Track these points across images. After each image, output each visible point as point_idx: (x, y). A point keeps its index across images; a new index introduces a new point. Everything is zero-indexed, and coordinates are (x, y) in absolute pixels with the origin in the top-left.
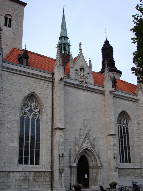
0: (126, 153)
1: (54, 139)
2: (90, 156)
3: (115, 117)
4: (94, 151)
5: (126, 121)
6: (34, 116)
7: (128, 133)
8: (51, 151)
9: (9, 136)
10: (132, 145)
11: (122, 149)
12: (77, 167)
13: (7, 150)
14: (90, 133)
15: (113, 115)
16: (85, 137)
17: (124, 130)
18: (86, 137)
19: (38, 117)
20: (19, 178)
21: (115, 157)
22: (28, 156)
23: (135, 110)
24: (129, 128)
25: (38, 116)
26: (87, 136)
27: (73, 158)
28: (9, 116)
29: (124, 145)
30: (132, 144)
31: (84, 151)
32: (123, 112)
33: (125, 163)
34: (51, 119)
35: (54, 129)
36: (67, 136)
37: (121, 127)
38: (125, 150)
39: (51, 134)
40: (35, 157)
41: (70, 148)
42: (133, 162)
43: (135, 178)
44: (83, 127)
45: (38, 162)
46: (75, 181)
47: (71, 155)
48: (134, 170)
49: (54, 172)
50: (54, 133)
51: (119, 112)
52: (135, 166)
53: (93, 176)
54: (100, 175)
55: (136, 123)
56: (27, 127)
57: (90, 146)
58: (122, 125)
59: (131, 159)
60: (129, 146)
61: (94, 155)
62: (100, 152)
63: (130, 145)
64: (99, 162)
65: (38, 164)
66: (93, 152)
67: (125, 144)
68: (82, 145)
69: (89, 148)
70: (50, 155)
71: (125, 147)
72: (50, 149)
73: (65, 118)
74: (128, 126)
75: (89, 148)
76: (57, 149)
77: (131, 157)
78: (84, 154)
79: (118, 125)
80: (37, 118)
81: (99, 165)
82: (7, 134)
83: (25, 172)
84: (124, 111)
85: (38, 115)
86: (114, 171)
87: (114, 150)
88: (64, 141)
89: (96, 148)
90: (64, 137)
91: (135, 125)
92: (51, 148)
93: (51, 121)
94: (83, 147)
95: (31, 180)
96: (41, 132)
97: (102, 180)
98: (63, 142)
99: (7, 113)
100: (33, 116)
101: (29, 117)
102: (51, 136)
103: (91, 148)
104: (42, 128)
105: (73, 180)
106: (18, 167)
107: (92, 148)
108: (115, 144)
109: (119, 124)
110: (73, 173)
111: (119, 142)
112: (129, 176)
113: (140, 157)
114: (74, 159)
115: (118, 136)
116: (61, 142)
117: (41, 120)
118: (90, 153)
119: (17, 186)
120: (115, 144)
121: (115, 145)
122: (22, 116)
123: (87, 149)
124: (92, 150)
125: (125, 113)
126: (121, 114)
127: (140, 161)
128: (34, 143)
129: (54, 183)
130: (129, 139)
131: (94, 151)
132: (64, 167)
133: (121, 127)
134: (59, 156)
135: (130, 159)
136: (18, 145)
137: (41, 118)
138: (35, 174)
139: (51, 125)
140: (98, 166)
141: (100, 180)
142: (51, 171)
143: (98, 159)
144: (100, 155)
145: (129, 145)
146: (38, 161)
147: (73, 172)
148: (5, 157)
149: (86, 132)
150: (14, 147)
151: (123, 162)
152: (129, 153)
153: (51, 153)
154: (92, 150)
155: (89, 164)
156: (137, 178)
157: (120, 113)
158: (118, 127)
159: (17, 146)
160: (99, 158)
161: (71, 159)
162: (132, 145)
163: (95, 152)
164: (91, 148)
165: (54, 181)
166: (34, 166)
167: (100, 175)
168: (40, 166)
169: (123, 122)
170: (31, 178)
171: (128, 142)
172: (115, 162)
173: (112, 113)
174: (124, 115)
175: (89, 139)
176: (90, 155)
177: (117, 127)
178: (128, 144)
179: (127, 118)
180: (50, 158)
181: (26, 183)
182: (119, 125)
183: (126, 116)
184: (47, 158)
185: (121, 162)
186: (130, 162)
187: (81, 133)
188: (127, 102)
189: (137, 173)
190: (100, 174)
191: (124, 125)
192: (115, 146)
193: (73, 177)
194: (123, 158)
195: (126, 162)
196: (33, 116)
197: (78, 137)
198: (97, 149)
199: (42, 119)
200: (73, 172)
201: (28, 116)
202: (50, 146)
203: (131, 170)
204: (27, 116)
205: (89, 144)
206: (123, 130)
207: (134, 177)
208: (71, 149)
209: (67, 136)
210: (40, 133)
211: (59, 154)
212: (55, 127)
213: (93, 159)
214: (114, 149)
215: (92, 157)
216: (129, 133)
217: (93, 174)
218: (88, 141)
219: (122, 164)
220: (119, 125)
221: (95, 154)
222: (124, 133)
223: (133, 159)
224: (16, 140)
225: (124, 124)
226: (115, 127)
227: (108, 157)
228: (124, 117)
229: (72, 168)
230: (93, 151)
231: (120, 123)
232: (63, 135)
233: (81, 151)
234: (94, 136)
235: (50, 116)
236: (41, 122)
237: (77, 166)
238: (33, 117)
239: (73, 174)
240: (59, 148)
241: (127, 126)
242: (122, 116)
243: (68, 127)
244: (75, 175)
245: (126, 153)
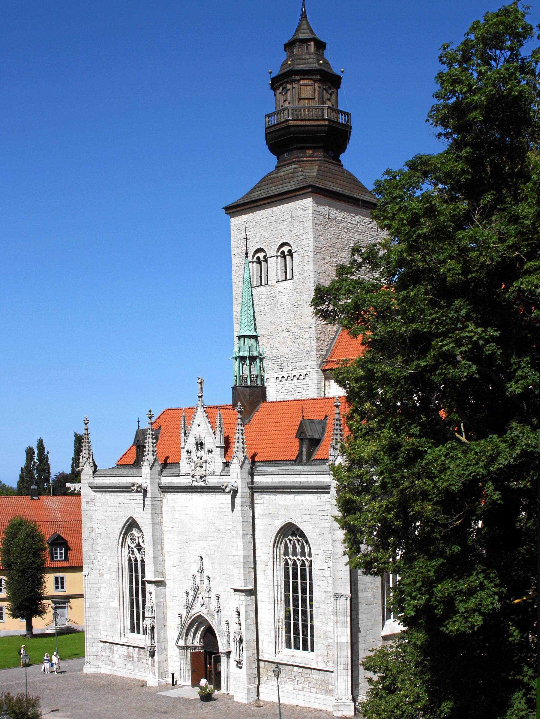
9: (109, 593)
11: (296, 617)
13: (109, 613)
17: (303, 570)
20: (123, 653)
23: (321, 517)
28: (109, 562)
29: (300, 609)
43: (309, 690)
48: (309, 671)
55: (321, 552)
71: (304, 613)
82: (107, 589)
83: (128, 646)
84: (290, 523)
91: (319, 557)
95: (136, 659)
99: (105, 558)
112: (293, 683)
113: (326, 643)
119: (121, 665)
127: (326, 652)
138: (139, 651)
148: (108, 622)
150: (115, 608)
156: (314, 690)
169: (303, 548)
170: (135, 655)
181: (130, 663)
188: (299, 497)
189: (314, 680)
203: (301, 670)
207: (306, 686)
225: (303, 554)
244: (182, 662)
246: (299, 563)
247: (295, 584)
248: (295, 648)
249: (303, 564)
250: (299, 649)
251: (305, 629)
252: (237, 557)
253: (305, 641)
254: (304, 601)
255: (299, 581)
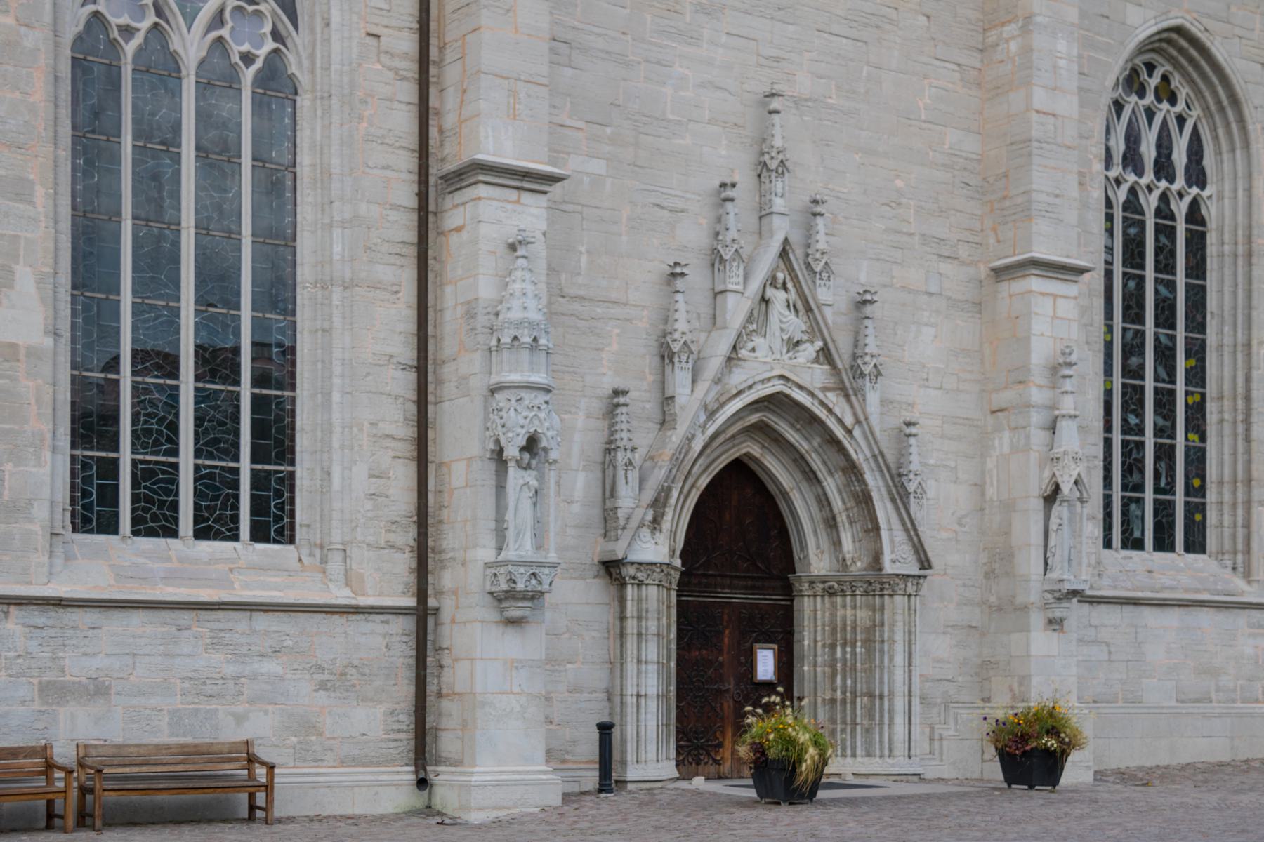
0: (1165, 454)
1: (448, 290)
2: (811, 477)
3: (1080, 89)
4: (849, 421)
5: (1195, 134)
6: (225, 32)
7: (1197, 268)
8: (413, 409)
10: (1227, 386)
11: (1133, 420)
12: (676, 576)
14: (821, 246)
15: (1062, 63)
16: (773, 282)
17: (1166, 233)
18: (780, 276)
19: (270, 45)
21: (1057, 489)
22: (175, 452)
24: (1210, 212)
25: (276, 35)
26: (791, 270)
27: (642, 481)
29: (1149, 384)
30: (1234, 378)
31: (754, 418)
32: (1169, 41)
33: (1149, 558)
34: (410, 68)
35: (445, 178)
36: (584, 259)
37: (1132, 204)
38: (1159, 432)
39: (412, 236)
40: (245, 465)
41: (609, 382)
42: (1227, 545)
44: (744, 178)
45: (278, 519)
46: (653, 705)
47: (620, 455)
49: (445, 615)
50: (452, 219)
51: (1132, 45)
52: (1240, 583)
53: (833, 667)
54: (899, 659)
56: (155, 154)
57: (817, 376)
58: (1144, 181)
59: (1212, 517)
60: (1203, 396)
61: (851, 470)
62: (912, 441)
63: (1211, 389)
64: (900, 536)
65: (280, 532)
66: (839, 433)
67: (1164, 375)
68: (732, 359)
69: (800, 387)
70: (409, 449)
71: (1165, 402)
72: (404, 383)
73: (568, 72)
74: (1205, 194)
75: (800, 387)
76: (479, 384)
77: (1211, 496)
78: (756, 450)
79: (1113, 174)
80: (258, 64)
81: (897, 558)
84: (1179, 30)
85: (267, 28)
86: (1037, 619)
87: (1055, 420)
88: (551, 314)
89: (873, 399)
90: (552, 270)
92: (412, 376)
93: (409, 91)
94: (738, 378)
96: (306, 213)
97: (916, 702)
98: (534, 316)
100: (214, 34)
101: (175, 44)
102: (413, 251)
103: (825, 389)
104: (313, 166)
105: (631, 701)
106: (59, 561)
107: (832, 398)
108: (1070, 365)
109: (1115, 172)
110: (639, 635)
111: (1109, 345)
114: (649, 495)
115: (1095, 280)
116: (516, 315)
117: (303, 79)
118: (816, 441)
120: (1070, 365)
121: (1067, 372)
122: (88, 25)
123: (776, 402)
124: (830, 410)
125: (1191, 60)
126: (1151, 68)
128: (237, 319)
129: (444, 723)
130: (1202, 328)
131: (858, 422)
132: (541, 565)
133: (1132, 204)
134: (499, 455)
135: (1196, 511)
136: (56, 334)
137: (306, 63)
139: (412, 141)
140: (889, 568)
141: (900, 704)
142: (411, 602)
143: (893, 500)
144: (913, 467)
145: (1202, 383)
146: (281, 507)
147: (639, 618)
149: (781, 229)
151: (1133, 542)
152: (1197, 460)
153: (411, 432)
154: (830, 410)
155: (803, 547)
157: (1143, 48)
158: (1109, 204)
159: (49, 341)
160: (900, 496)
161: (613, 494)
162: (1227, 386)
163: (857, 433)
164: (825, 389)
165: (446, 704)
166: (244, 551)
167: (899, 659)
168: (306, 560)
169: (1164, 146)
171: (1197, 351)
172: (1052, 543)
173: (1062, 46)
174: (1176, 81)
175: (806, 307)
176: (816, 463)
177: (1097, 195)
178: (1197, 376)
179: (1206, 109)
180: (403, 476)
182: (1118, 182)
183: (1198, 92)
184: (371, 476)
185: (1108, 544)
186: (1196, 544)
187: (732, 234)
190: (899, 648)
191: (1163, 184)
192: (1068, 385)
193: (631, 667)
194: (1133, 507)
195: (1164, 542)
196: (214, 34)
197: (697, 278)
198: (884, 402)
199: (312, 72)
200: (631, 625)
201: (156, 25)
202: (408, 354)
204: (145, 25)
205: (809, 350)
206: (1159, 229)
208: (617, 393)
209: (584, 259)
210: (294, 225)
211: (497, 442)
212: (449, 156)
213: (837, 504)
214: (1053, 407)
215: (831, 485)
216: (1211, 264)
217: (833, 647)
218: (797, 325)
219: (1119, 557)
220: (1118, 182)
221: (859, 453)
222: (1165, 264)
223: (1227, 519)
224: (25, 279)
225: (1164, 168)
226: (1074, 192)
227: (991, 492)
228: (1173, 100)
229: (622, 585)
230: (840, 421)
231: (1132, 159)
232: (539, 249)
233: (721, 418)
234: (863, 278)
235: (407, 43)
236: (304, 101)
237: (678, 562)
238: (220, 40)
239: (631, 644)
240: (495, 379)
241: (1195, 190)
242: (1154, 81)
243: (598, 167)
245: (1165, 454)
246: (1150, 203)
247: (1132, 284)
248: (1125, 545)
249: (1164, 211)
250: (1138, 545)
251: (1163, 466)
252: (1051, 120)
253: (1164, 511)
254: (1165, 355)
255: (1150, 273)
